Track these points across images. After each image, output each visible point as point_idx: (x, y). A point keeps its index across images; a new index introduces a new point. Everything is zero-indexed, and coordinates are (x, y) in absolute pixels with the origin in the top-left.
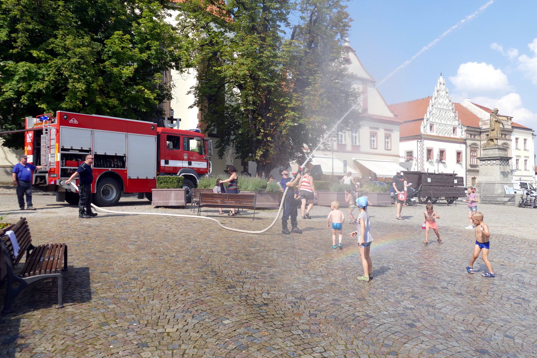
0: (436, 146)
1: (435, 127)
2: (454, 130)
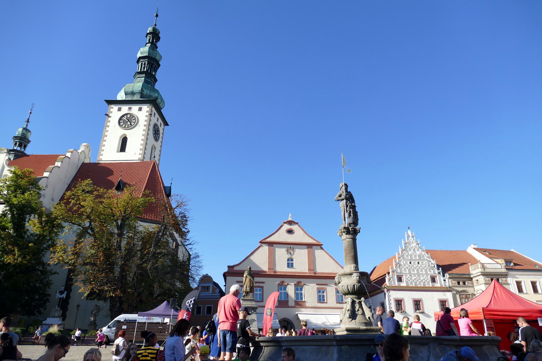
0: (408, 298)
1: (404, 278)
2: (433, 280)
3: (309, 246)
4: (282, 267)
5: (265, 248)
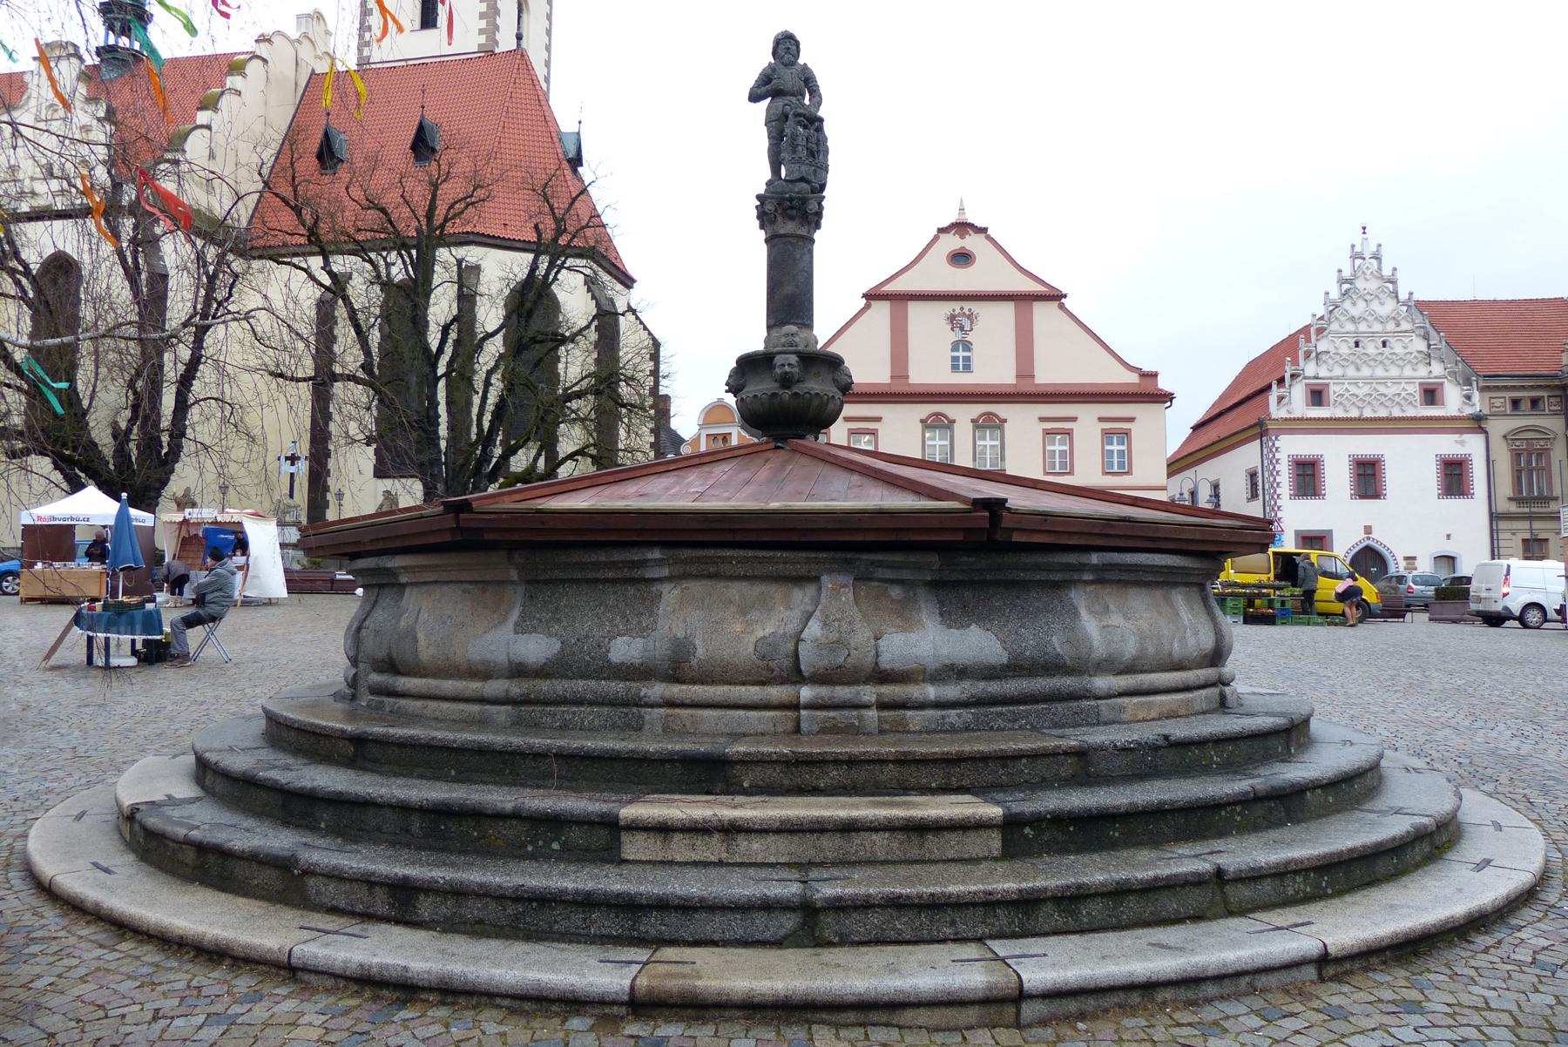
2: (1431, 395)
3: (1022, 300)
4: (931, 368)
5: (882, 310)
